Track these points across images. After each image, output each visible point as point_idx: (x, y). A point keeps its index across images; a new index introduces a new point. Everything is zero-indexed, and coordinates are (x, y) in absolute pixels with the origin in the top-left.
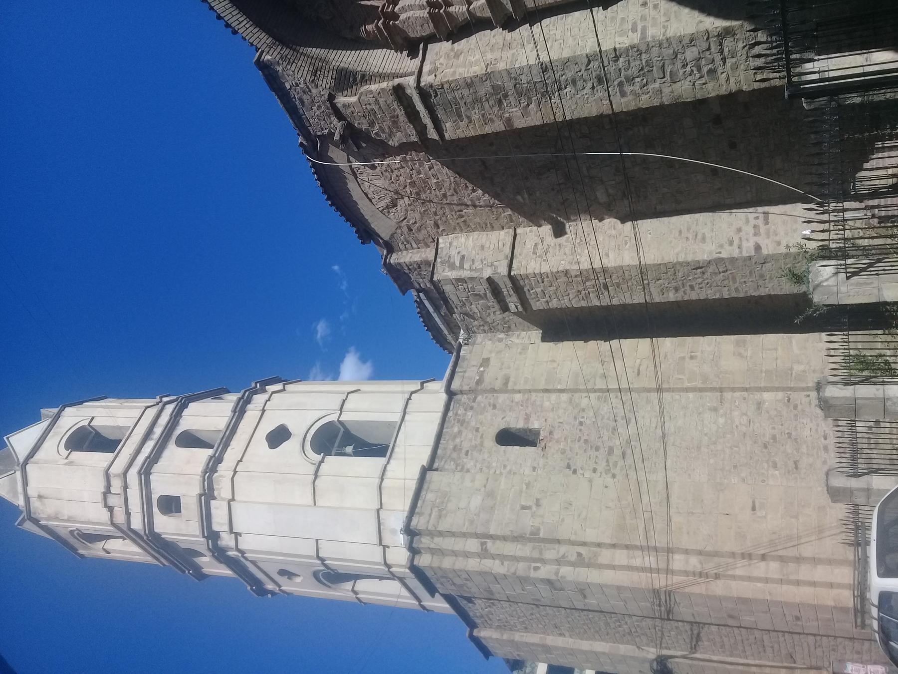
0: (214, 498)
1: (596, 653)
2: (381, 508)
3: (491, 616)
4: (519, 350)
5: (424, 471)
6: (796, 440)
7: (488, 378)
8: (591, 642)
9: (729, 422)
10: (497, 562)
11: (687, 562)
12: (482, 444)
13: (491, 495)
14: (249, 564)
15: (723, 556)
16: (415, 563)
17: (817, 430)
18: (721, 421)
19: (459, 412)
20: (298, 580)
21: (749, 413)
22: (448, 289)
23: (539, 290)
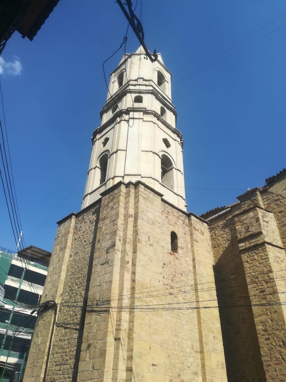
0: (144, 114)
1: (60, 272)
2: (141, 177)
3: (84, 223)
4: (208, 250)
5: (161, 195)
7: (197, 232)
8: (66, 270)
10: (123, 222)
11: (125, 321)
12: (171, 225)
13: (153, 223)
14: (113, 125)
15: (129, 343)
16: (122, 185)
18: (188, 350)
19: (182, 217)
20: (102, 146)
22: (251, 214)
23: (256, 257)
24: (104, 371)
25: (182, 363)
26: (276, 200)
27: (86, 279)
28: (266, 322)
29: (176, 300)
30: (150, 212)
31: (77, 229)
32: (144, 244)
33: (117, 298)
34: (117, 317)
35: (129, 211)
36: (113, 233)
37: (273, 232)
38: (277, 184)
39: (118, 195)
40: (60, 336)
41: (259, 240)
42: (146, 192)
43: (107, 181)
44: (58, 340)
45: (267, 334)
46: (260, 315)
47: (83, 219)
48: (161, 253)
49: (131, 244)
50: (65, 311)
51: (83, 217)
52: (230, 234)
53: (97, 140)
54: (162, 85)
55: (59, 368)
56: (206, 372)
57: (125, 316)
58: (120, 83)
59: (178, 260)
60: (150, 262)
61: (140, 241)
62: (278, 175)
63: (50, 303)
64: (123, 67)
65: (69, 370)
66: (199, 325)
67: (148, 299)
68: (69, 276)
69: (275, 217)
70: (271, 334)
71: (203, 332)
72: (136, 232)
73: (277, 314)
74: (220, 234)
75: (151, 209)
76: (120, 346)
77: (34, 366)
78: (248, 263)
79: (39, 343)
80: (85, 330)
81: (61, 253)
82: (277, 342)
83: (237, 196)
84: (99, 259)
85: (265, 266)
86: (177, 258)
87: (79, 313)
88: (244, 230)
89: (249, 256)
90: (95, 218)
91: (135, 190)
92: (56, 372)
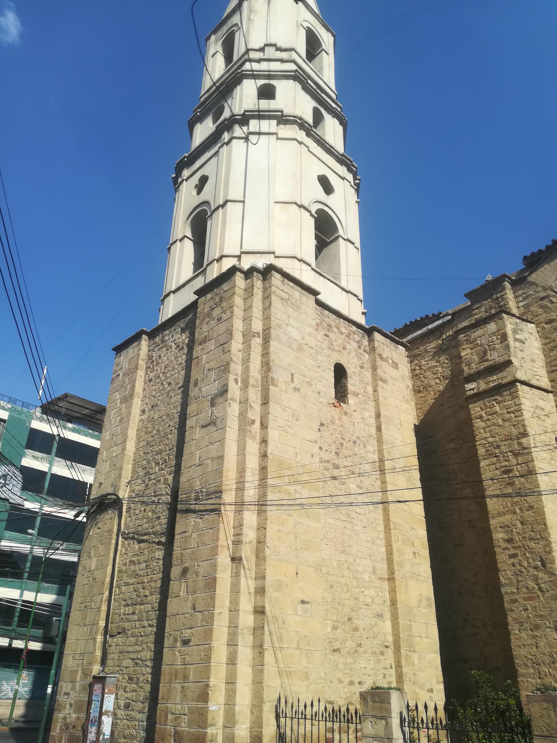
0: (278, 124)
1: (124, 442)
2: (275, 257)
6: (356, 651)
7: (384, 364)
8: (135, 438)
9: (366, 584)
10: (241, 347)
11: (250, 528)
12: (333, 350)
13: (300, 348)
14: (216, 149)
15: (257, 565)
16: (238, 273)
17: (365, 674)
18: (366, 577)
20: (194, 193)
21: (373, 606)
22: (492, 327)
23: (497, 408)
24: (213, 614)
25: (355, 598)
26: (542, 299)
27: (174, 453)
28: (512, 526)
29: (344, 489)
30: (293, 327)
31: (152, 362)
32: (283, 388)
33: (234, 487)
34: (234, 521)
35: (252, 324)
36: (223, 367)
37: (533, 361)
38: (546, 266)
39: (230, 293)
40: (130, 555)
41: (504, 377)
42: (285, 288)
43: (207, 265)
44: (128, 563)
45: (513, 547)
46: (500, 514)
47: (163, 341)
48: (315, 404)
49: (258, 388)
50: (137, 511)
51: (163, 337)
52: (449, 367)
53: (183, 180)
54: (317, 59)
55: (131, 611)
56: (398, 612)
57: (250, 518)
58: (228, 57)
59: (349, 416)
60: (294, 421)
61: (275, 382)
62: (548, 247)
63: (109, 497)
64: (235, 19)
65: (151, 613)
66: (386, 533)
67: (292, 488)
68: (141, 449)
69: (538, 332)
70: (520, 547)
71: (393, 544)
72: (266, 366)
73: (533, 511)
74: (429, 366)
75: (294, 321)
76: (242, 571)
77: (85, 607)
78: (481, 420)
79: (93, 568)
80: (176, 544)
81: (125, 407)
82: (531, 560)
83: (466, 292)
84: (197, 416)
85: (514, 425)
86: (346, 413)
87: (165, 514)
88: (476, 357)
89: (484, 408)
90: (187, 339)
91: (264, 284)
92: (128, 616)
